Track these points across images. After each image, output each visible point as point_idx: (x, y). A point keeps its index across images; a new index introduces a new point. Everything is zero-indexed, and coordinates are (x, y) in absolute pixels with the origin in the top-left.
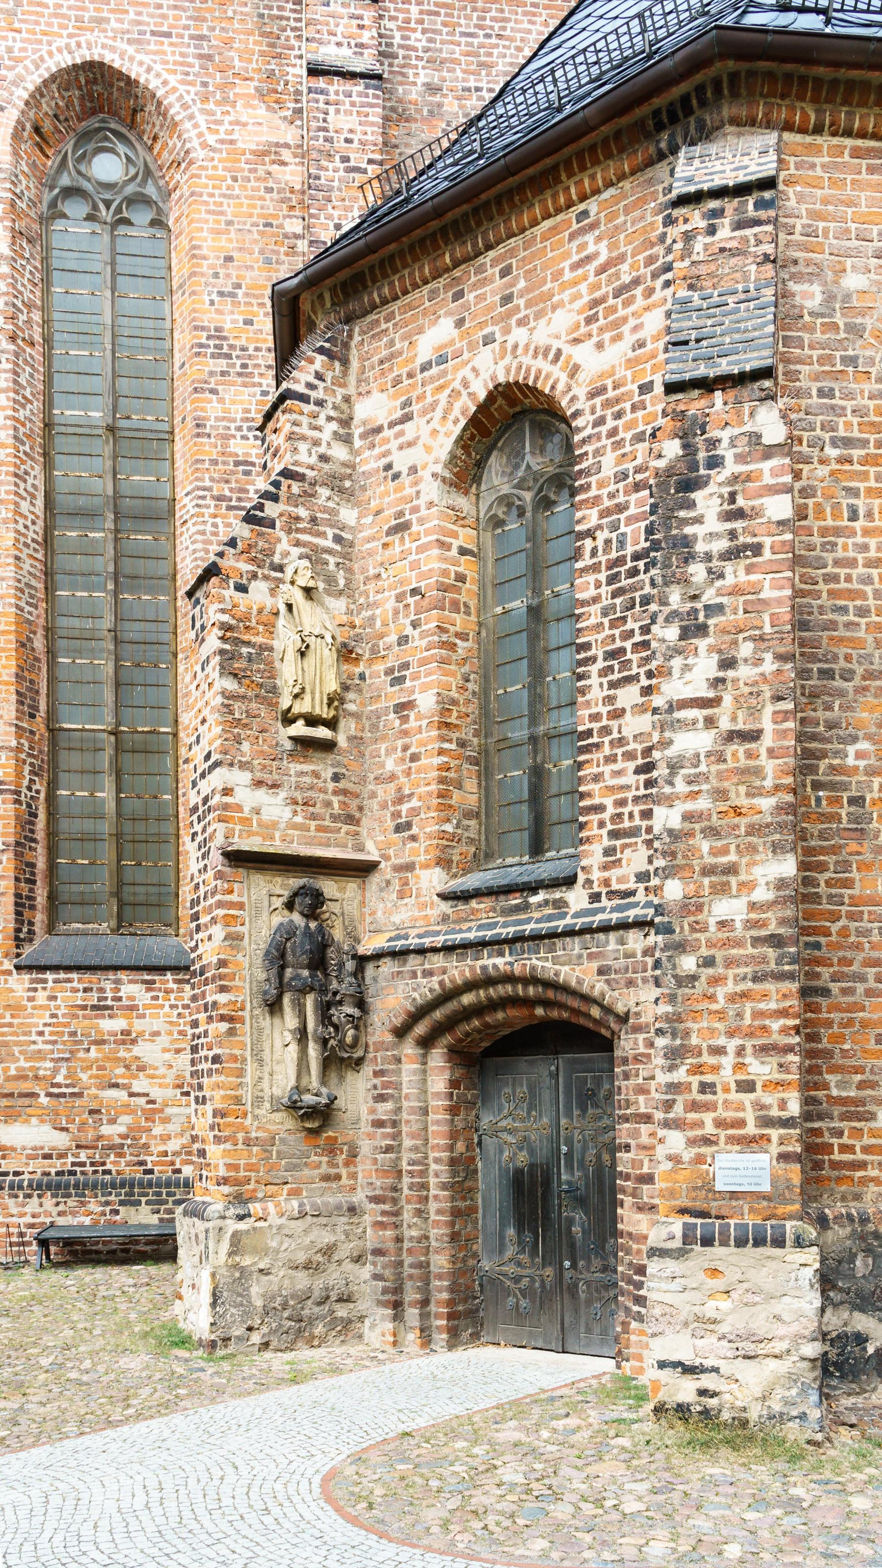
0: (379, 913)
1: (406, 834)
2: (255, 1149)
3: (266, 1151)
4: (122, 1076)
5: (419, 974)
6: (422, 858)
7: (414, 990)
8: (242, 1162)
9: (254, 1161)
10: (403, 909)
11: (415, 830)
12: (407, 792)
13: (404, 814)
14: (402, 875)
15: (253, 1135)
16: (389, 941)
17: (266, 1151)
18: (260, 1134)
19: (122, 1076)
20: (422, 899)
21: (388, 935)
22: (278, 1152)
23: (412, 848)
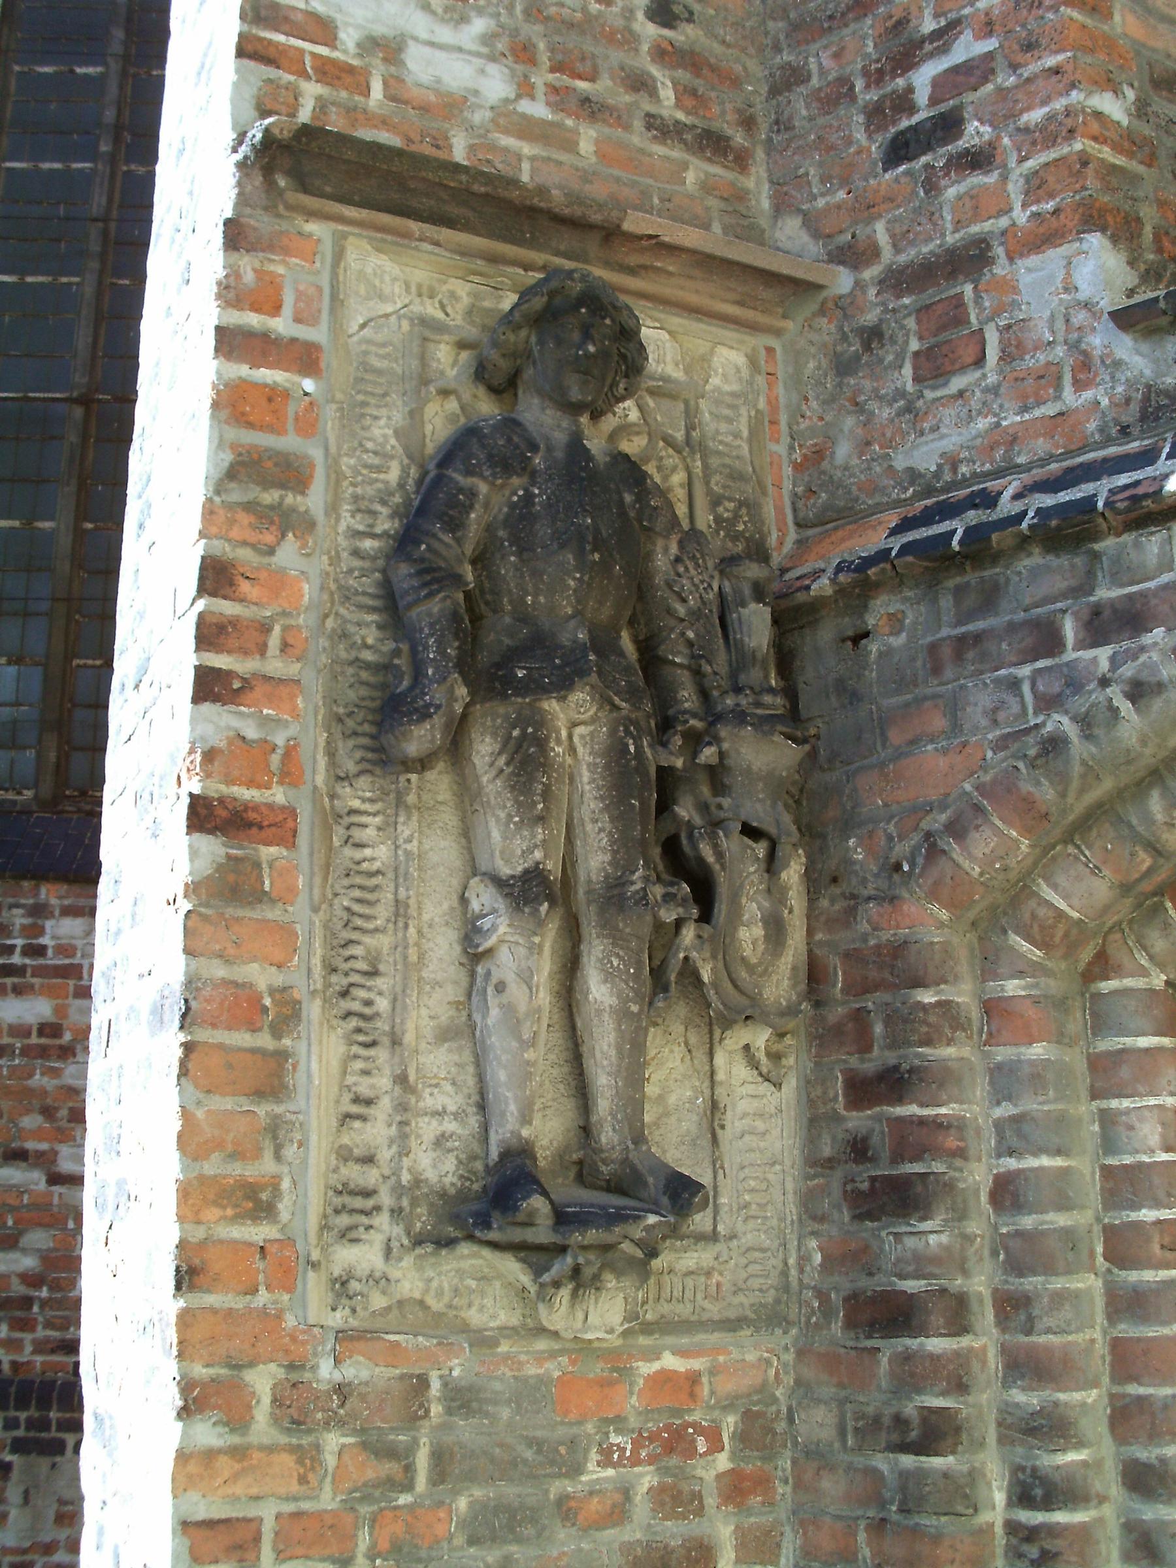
0: (843, 451)
1: (937, 158)
2: (333, 1441)
3: (390, 1453)
4: (38, 1134)
5: (1069, 630)
6: (1021, 216)
7: (1047, 703)
8: (268, 1513)
9: (327, 1500)
10: (948, 414)
11: (975, 132)
12: (929, 25)
13: (922, 96)
14: (931, 295)
15: (326, 1371)
16: (894, 532)
17: (390, 1453)
18: (356, 1370)
19: (38, 1134)
20: (1035, 361)
21: (892, 519)
22: (439, 1457)
23: (972, 195)
